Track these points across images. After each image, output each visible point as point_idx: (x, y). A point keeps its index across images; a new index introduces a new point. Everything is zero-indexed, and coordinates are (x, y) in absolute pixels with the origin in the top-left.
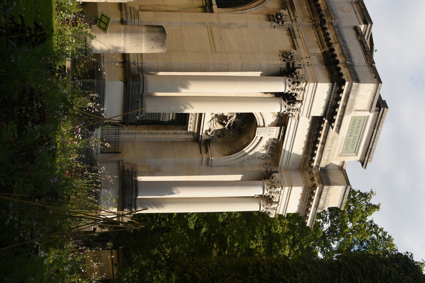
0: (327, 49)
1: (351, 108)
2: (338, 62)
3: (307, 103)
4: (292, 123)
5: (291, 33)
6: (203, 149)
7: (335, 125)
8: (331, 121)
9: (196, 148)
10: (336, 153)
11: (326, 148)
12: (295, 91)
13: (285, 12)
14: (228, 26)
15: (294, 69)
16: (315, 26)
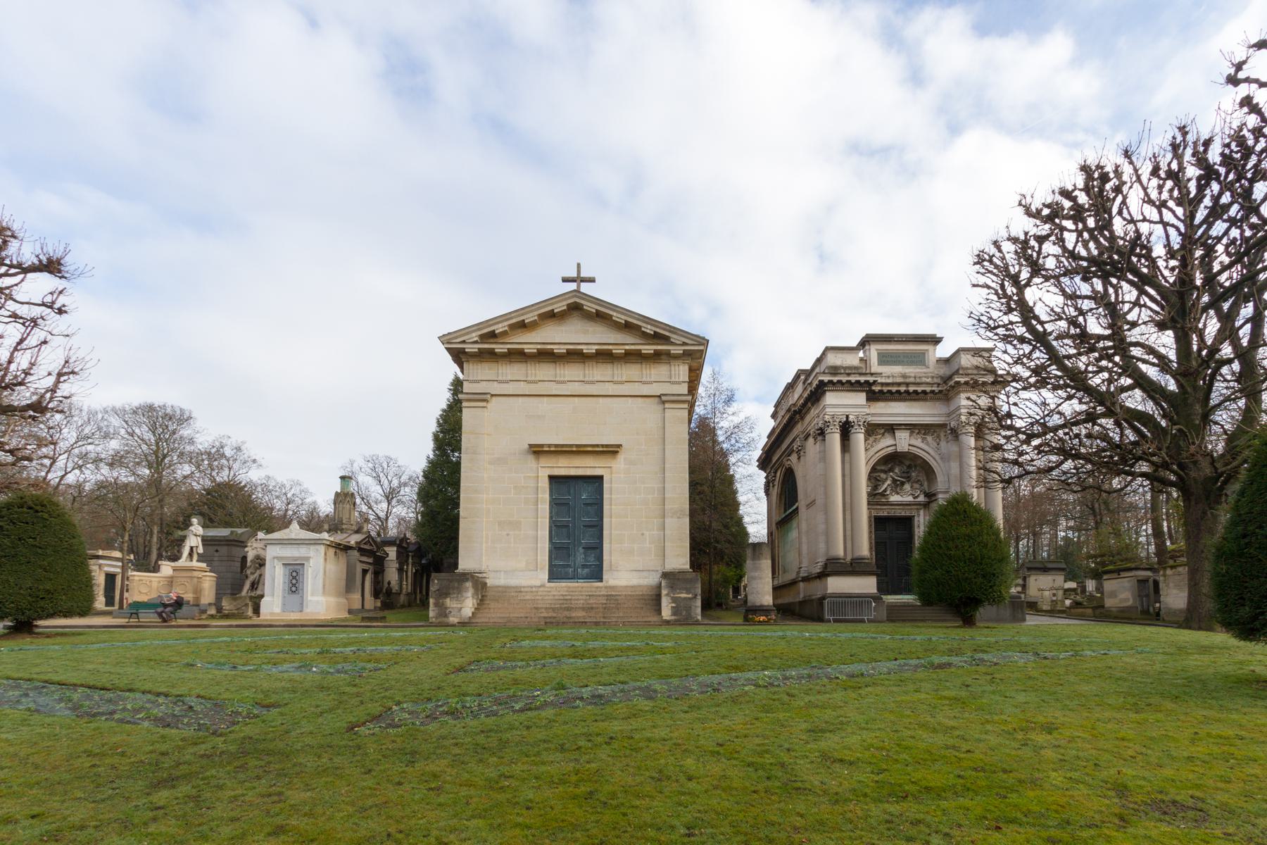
7: (871, 379)
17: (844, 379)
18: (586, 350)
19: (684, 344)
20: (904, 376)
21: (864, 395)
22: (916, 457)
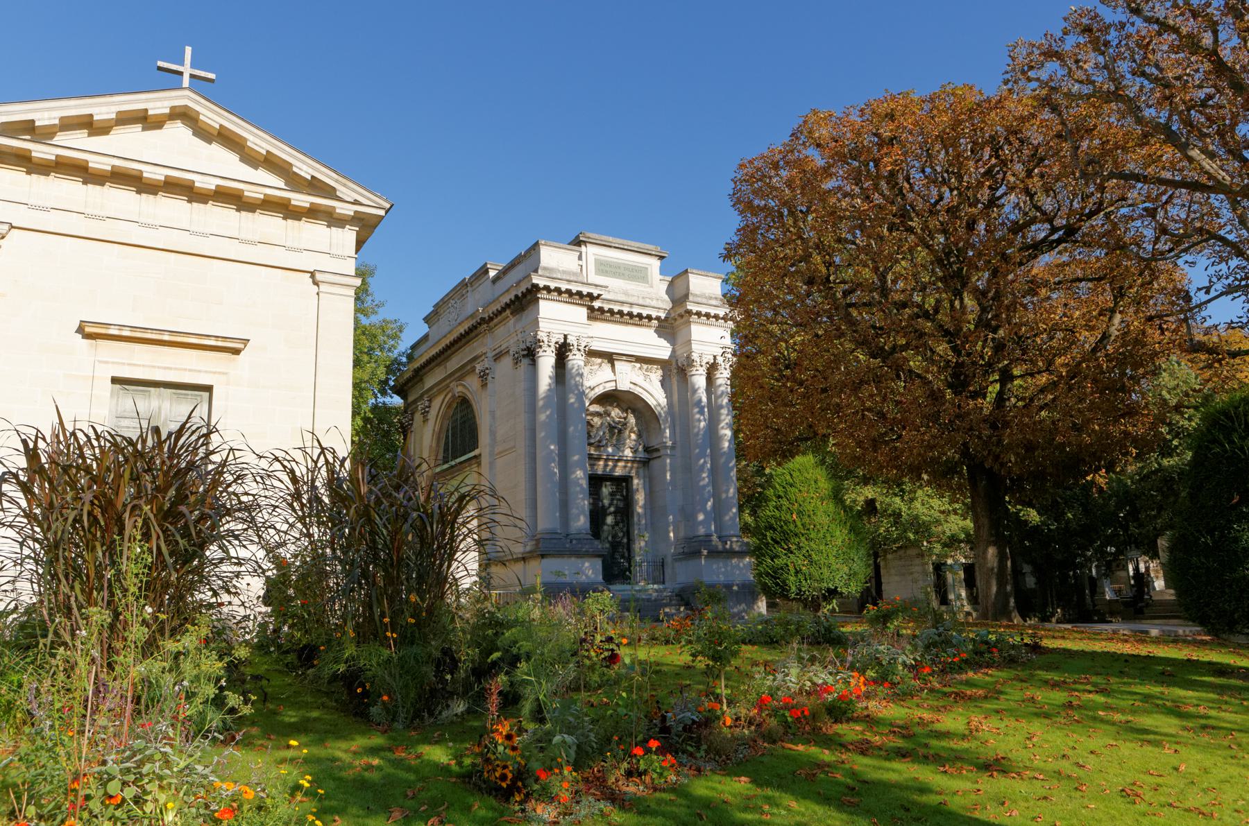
0: (508, 312)
1: (575, 274)
2: (516, 296)
4: (597, 346)
5: (498, 357)
6: (655, 455)
7: (595, 292)
8: (591, 297)
9: (654, 463)
10: (649, 290)
11: (641, 302)
12: (552, 344)
13: (479, 367)
14: (493, 433)
15: (528, 349)
16: (491, 329)
17: (564, 287)
18: (201, 183)
19: (356, 203)
20: (626, 293)
21: (583, 312)
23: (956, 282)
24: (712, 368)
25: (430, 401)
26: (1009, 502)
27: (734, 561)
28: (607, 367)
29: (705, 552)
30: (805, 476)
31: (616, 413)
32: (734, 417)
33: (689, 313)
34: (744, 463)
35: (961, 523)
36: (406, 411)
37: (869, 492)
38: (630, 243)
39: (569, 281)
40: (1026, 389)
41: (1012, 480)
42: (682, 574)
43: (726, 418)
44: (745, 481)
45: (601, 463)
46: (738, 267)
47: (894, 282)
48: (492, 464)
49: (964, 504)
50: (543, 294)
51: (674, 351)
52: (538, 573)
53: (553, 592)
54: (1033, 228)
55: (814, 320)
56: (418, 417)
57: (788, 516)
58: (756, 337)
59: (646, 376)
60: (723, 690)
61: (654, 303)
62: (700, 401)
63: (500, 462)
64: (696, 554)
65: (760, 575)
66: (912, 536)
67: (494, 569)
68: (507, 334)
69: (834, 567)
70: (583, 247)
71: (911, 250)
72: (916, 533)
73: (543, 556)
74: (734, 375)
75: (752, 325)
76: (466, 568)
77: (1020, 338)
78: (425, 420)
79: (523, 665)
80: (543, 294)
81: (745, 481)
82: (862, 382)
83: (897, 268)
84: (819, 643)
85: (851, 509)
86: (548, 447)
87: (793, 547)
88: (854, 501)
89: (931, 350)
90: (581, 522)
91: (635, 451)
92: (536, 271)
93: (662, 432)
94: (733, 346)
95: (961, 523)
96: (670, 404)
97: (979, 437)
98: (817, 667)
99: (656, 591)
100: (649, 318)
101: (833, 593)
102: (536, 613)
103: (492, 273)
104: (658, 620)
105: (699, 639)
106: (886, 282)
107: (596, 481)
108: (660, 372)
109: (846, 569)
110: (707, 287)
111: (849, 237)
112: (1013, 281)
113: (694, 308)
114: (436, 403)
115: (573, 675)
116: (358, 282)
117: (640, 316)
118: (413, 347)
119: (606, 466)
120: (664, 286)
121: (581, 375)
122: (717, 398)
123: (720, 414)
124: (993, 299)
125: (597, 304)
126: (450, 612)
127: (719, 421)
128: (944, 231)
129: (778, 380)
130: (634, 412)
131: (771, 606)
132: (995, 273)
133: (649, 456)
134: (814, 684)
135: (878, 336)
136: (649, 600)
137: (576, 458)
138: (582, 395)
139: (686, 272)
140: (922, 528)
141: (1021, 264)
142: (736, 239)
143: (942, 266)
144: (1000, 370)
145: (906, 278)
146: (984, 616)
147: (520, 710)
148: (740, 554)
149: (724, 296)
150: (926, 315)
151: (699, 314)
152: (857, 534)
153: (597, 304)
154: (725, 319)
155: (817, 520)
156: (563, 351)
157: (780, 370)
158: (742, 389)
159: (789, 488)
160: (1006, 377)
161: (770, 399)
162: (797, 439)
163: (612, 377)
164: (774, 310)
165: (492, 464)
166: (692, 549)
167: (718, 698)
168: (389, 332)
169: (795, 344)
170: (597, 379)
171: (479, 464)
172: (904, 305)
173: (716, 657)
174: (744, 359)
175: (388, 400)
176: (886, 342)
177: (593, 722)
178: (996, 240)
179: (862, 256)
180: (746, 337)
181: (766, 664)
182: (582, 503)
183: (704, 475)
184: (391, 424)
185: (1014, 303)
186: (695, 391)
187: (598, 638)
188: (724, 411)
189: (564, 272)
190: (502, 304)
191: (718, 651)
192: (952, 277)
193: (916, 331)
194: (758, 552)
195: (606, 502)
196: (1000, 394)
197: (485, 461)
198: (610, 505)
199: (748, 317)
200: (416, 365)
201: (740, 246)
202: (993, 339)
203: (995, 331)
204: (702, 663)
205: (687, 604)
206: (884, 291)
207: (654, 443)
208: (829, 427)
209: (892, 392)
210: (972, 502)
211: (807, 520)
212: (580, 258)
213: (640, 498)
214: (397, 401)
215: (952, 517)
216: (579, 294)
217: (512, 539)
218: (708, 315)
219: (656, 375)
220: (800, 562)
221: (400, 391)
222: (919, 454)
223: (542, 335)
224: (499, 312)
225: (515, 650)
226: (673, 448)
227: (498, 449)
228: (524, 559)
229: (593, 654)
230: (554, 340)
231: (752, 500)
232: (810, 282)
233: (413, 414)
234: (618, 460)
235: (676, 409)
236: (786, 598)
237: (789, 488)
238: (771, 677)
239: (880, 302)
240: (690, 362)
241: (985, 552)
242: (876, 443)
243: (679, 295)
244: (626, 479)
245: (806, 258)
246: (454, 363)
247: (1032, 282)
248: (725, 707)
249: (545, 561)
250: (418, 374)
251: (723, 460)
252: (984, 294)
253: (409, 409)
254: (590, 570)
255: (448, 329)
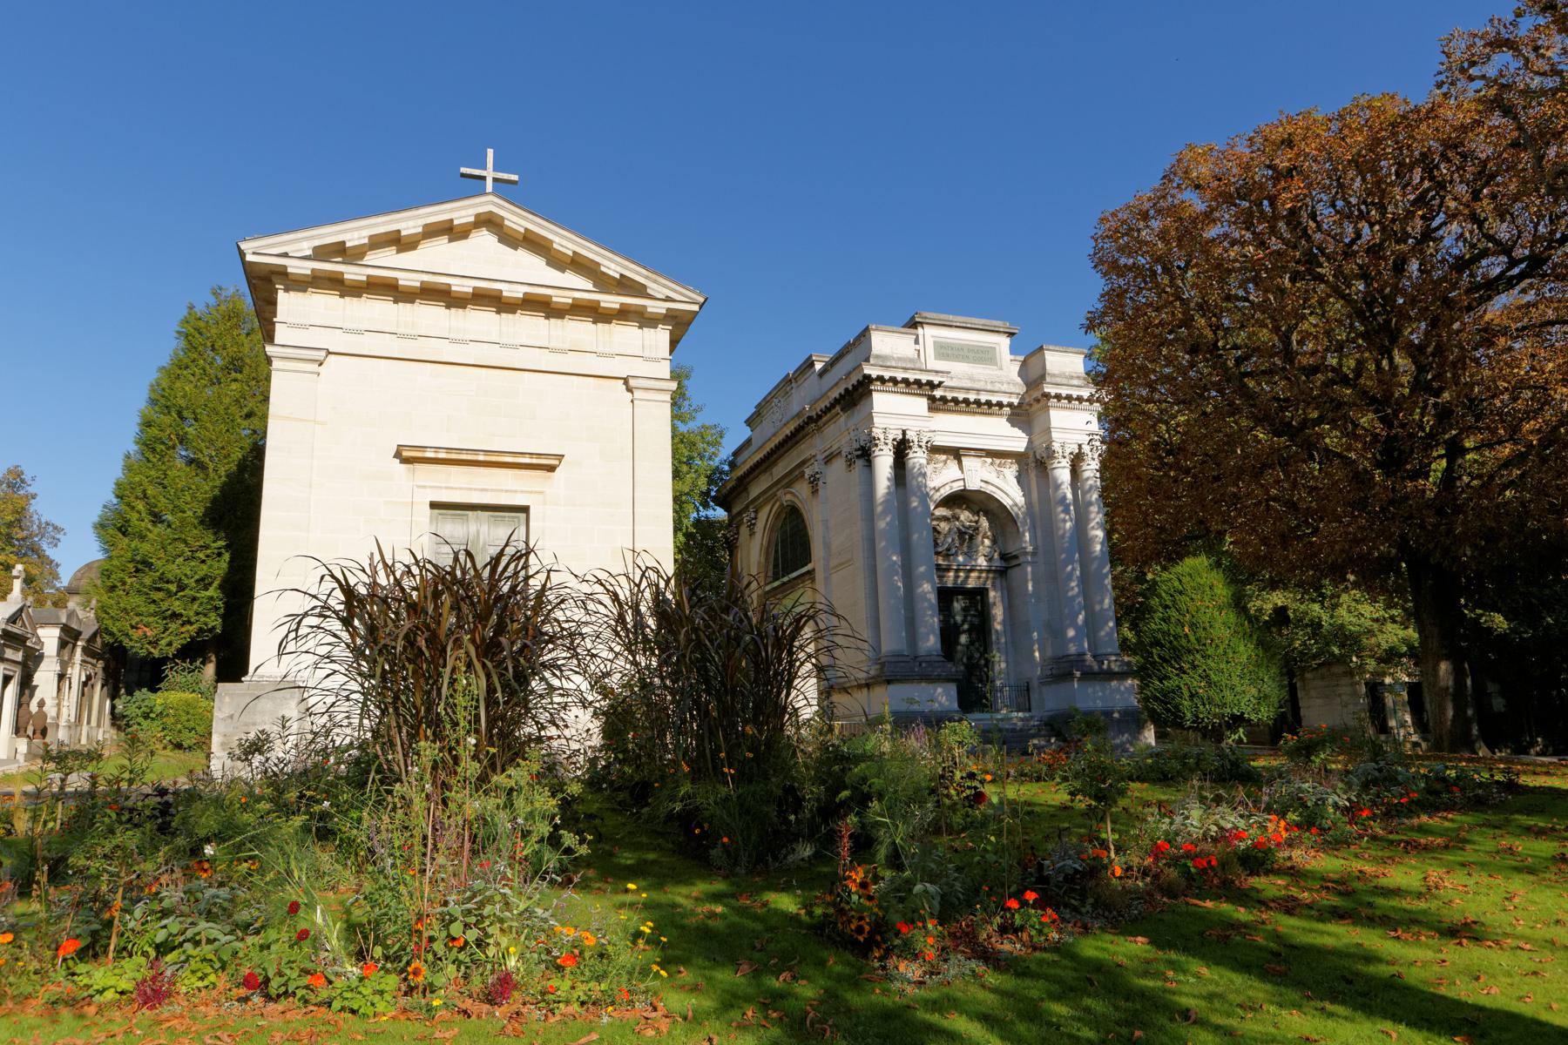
0: (838, 408)
1: (911, 360)
3: (905, 424)
4: (940, 441)
5: (828, 460)
6: (1014, 562)
7: (936, 380)
8: (932, 385)
9: (1014, 573)
10: (999, 373)
11: (989, 387)
13: (808, 472)
14: (827, 545)
15: (862, 448)
16: (819, 429)
17: (900, 375)
20: (971, 379)
21: (924, 402)
22: (990, 497)
23: (1383, 337)
24: (1077, 460)
25: (756, 512)
26: (1466, 606)
27: (1114, 683)
28: (953, 464)
29: (1078, 674)
30: (1198, 583)
31: (965, 516)
32: (1106, 515)
33: (1047, 396)
34: (1120, 568)
35: (1402, 633)
36: (730, 524)
37: (1278, 598)
38: (976, 321)
39: (905, 369)
40: (1483, 464)
41: (1468, 578)
42: (1051, 700)
43: (1096, 516)
44: (1122, 589)
45: (951, 574)
46: (1103, 339)
47: (1301, 343)
48: (827, 579)
49: (1404, 609)
50: (877, 386)
51: (1030, 442)
52: (885, 700)
53: (904, 722)
54: (1484, 262)
55: (1201, 396)
56: (744, 530)
57: (1179, 630)
58: (1129, 419)
59: (999, 473)
60: (1110, 836)
61: (1004, 388)
62: (1064, 497)
63: (835, 578)
64: (1066, 676)
65: (1146, 699)
66: (1336, 650)
67: (836, 698)
68: (838, 434)
69: (1238, 689)
70: (920, 330)
71: (1321, 303)
72: (1342, 646)
73: (889, 682)
74: (1104, 468)
75: (1123, 406)
76: (805, 697)
77: (1472, 401)
78: (752, 534)
79: (875, 805)
80: (877, 386)
81: (1122, 589)
82: (1264, 466)
83: (1305, 326)
84: (1224, 780)
85: (1257, 619)
86: (889, 558)
87: (1186, 666)
88: (1260, 610)
89: (1353, 422)
90: (931, 642)
91: (990, 560)
92: (867, 360)
93: (1019, 535)
94: (1101, 432)
95: (1402, 633)
96: (1029, 503)
97: (1422, 526)
98: (1223, 808)
99: (1022, 719)
100: (1000, 405)
101: (1238, 720)
102: (886, 747)
103: (818, 366)
104: (1025, 753)
105: (1076, 776)
106: (1290, 343)
107: (946, 596)
108: (1015, 467)
109: (1254, 691)
110: (1067, 365)
111: (1241, 293)
112: (1459, 331)
113: (1052, 390)
114: (763, 515)
115: (931, 817)
116: (674, 385)
117: (989, 403)
118: (735, 454)
119: (957, 577)
120: (1016, 367)
121: (924, 475)
122: (1084, 494)
123: (1088, 513)
124: (1433, 355)
125: (938, 393)
126: (790, 745)
127: (1088, 521)
128: (1364, 276)
129: (1158, 470)
130: (986, 514)
131: (1160, 736)
132: (1434, 323)
133: (1006, 566)
134: (1221, 828)
135: (1283, 409)
136: (1013, 730)
137: (922, 569)
138: (925, 497)
139: (1041, 348)
140: (1350, 640)
141: (1469, 309)
142: (1099, 306)
143: (1363, 320)
144: (1445, 442)
145: (1316, 337)
146: (1437, 746)
147: (874, 855)
148: (1122, 676)
149: (1088, 373)
150: (1345, 381)
151: (1058, 397)
152: (1266, 650)
153: (938, 393)
154: (1090, 400)
155: (1215, 633)
156: (902, 448)
157: (1161, 458)
158: (1115, 481)
159: (1178, 597)
160: (1455, 451)
161: (1150, 492)
162: (1186, 538)
163: (959, 475)
164: (1152, 387)
165: (827, 579)
166: (1063, 669)
167: (1104, 844)
168: (709, 438)
169: (1178, 425)
170: (943, 478)
171: (813, 580)
172: (1315, 370)
173: (1100, 796)
174: (1114, 447)
175: (710, 513)
176: (1292, 416)
177: (959, 869)
178: (1432, 281)
179: (1258, 315)
180: (1117, 420)
181: (1160, 804)
182: (931, 621)
183: (1073, 584)
184: (716, 540)
185: (1462, 359)
186: (1058, 486)
187: (958, 775)
188: (1094, 509)
189: (900, 359)
190: (831, 400)
191: (1102, 788)
192: (1377, 332)
193: (1332, 400)
194: (1143, 673)
195: (959, 619)
196: (1448, 471)
197: (819, 576)
198: (964, 621)
199: (1119, 396)
200: (740, 472)
201: (1104, 314)
202: (1435, 405)
203: (1437, 394)
204: (1082, 803)
205: (1059, 735)
206: (1288, 355)
207: (1012, 549)
208: (1224, 522)
209: (1304, 476)
210: (1415, 606)
211: (1201, 633)
212: (917, 342)
213: (998, 613)
214: (719, 514)
215: (1389, 626)
216: (918, 383)
217: (854, 661)
218: (1069, 398)
219: (1011, 471)
220: (1193, 681)
221: (723, 502)
222: (1342, 551)
223: (877, 432)
224: (827, 410)
225: (865, 789)
226: (1034, 554)
227: (833, 563)
228: (868, 686)
229: (953, 792)
230: (891, 437)
231: (1132, 610)
232: (1193, 350)
233: (738, 528)
234: (971, 570)
235: (1037, 508)
236: (1181, 726)
237: (1178, 597)
238: (1167, 820)
239: (1284, 369)
240: (1051, 454)
241: (1436, 669)
242: (1285, 539)
243: (1034, 376)
244: (981, 592)
245: (1187, 322)
246: (780, 470)
247: (1485, 330)
248: (1113, 855)
249: (892, 687)
250: (743, 483)
251: (1095, 566)
252: (1421, 348)
253: (734, 522)
254: (943, 697)
255: (773, 430)
